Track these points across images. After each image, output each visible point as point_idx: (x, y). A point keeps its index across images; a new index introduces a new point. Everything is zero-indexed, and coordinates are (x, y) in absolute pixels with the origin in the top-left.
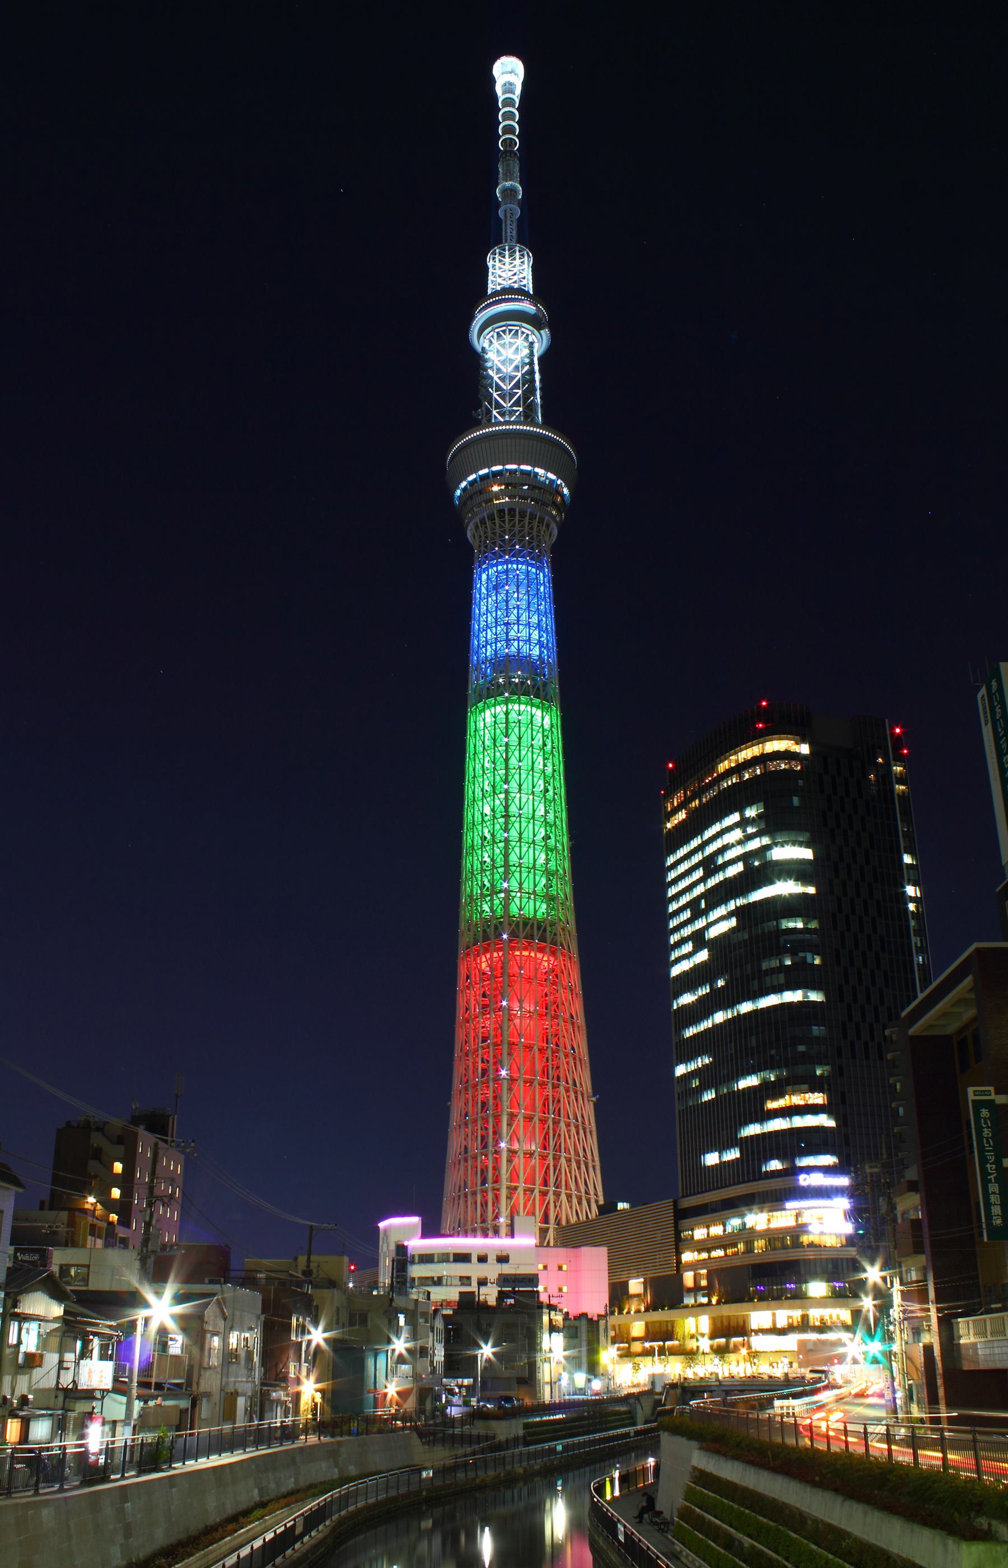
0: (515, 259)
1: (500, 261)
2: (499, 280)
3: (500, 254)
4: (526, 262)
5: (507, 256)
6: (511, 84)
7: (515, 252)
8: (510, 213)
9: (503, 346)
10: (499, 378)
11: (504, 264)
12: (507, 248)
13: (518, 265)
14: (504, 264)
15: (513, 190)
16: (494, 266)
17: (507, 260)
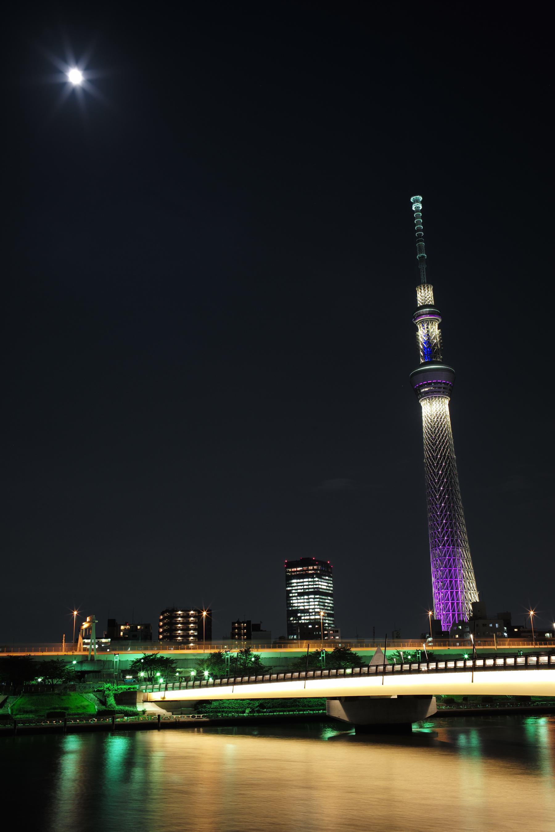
0: (425, 291)
1: (420, 292)
2: (420, 300)
3: (421, 289)
4: (430, 290)
5: (422, 290)
6: (418, 207)
7: (425, 287)
8: (423, 268)
9: (424, 329)
10: (424, 342)
11: (421, 293)
12: (422, 286)
13: (427, 293)
14: (421, 293)
15: (423, 257)
16: (418, 293)
17: (423, 291)
